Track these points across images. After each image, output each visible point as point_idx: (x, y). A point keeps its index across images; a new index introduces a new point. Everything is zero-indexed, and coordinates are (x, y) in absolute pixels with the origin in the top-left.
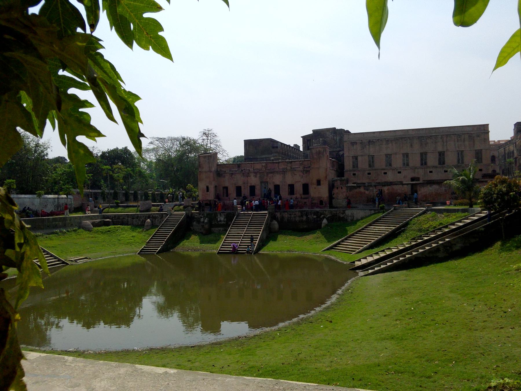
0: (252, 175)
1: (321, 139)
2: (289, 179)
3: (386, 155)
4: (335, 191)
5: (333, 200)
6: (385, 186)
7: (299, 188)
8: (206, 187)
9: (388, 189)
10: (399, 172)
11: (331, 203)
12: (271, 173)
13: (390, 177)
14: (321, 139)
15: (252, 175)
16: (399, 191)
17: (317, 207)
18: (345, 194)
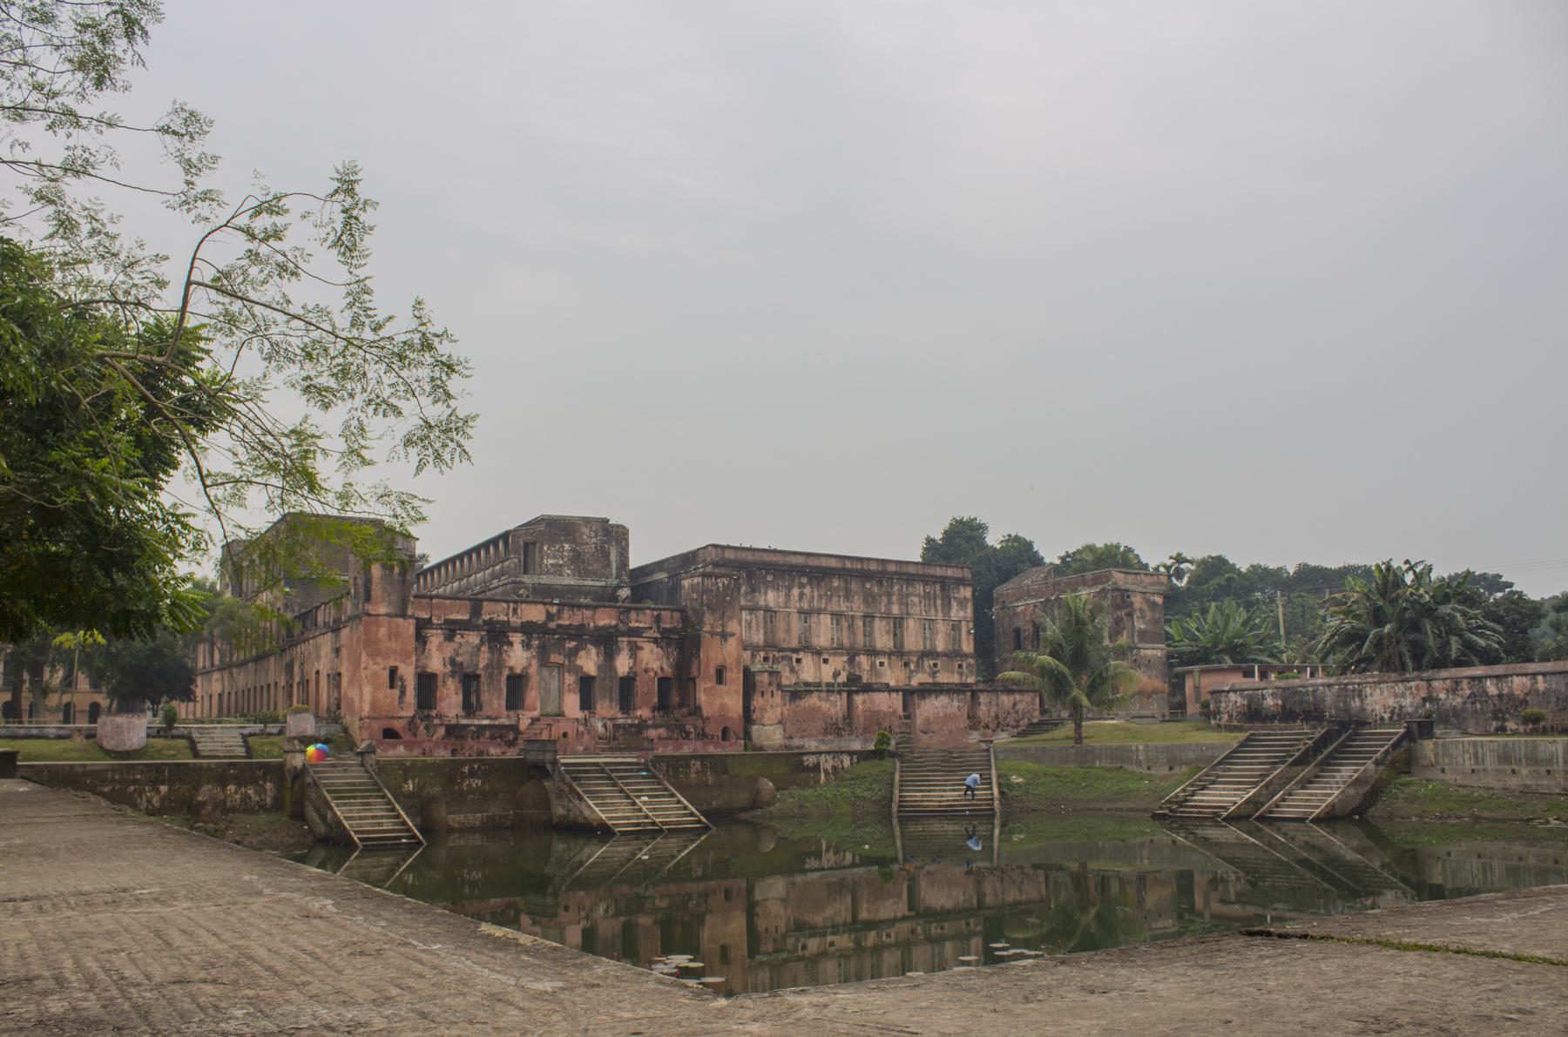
0: (517, 638)
1: (567, 546)
2: (623, 664)
3: (801, 612)
4: (757, 701)
5: (755, 728)
6: (857, 692)
7: (647, 690)
8: (386, 674)
9: (864, 702)
10: (826, 661)
11: (747, 735)
12: (572, 637)
13: (809, 670)
14: (567, 546)
15: (517, 638)
16: (884, 708)
17: (717, 745)
18: (779, 711)
